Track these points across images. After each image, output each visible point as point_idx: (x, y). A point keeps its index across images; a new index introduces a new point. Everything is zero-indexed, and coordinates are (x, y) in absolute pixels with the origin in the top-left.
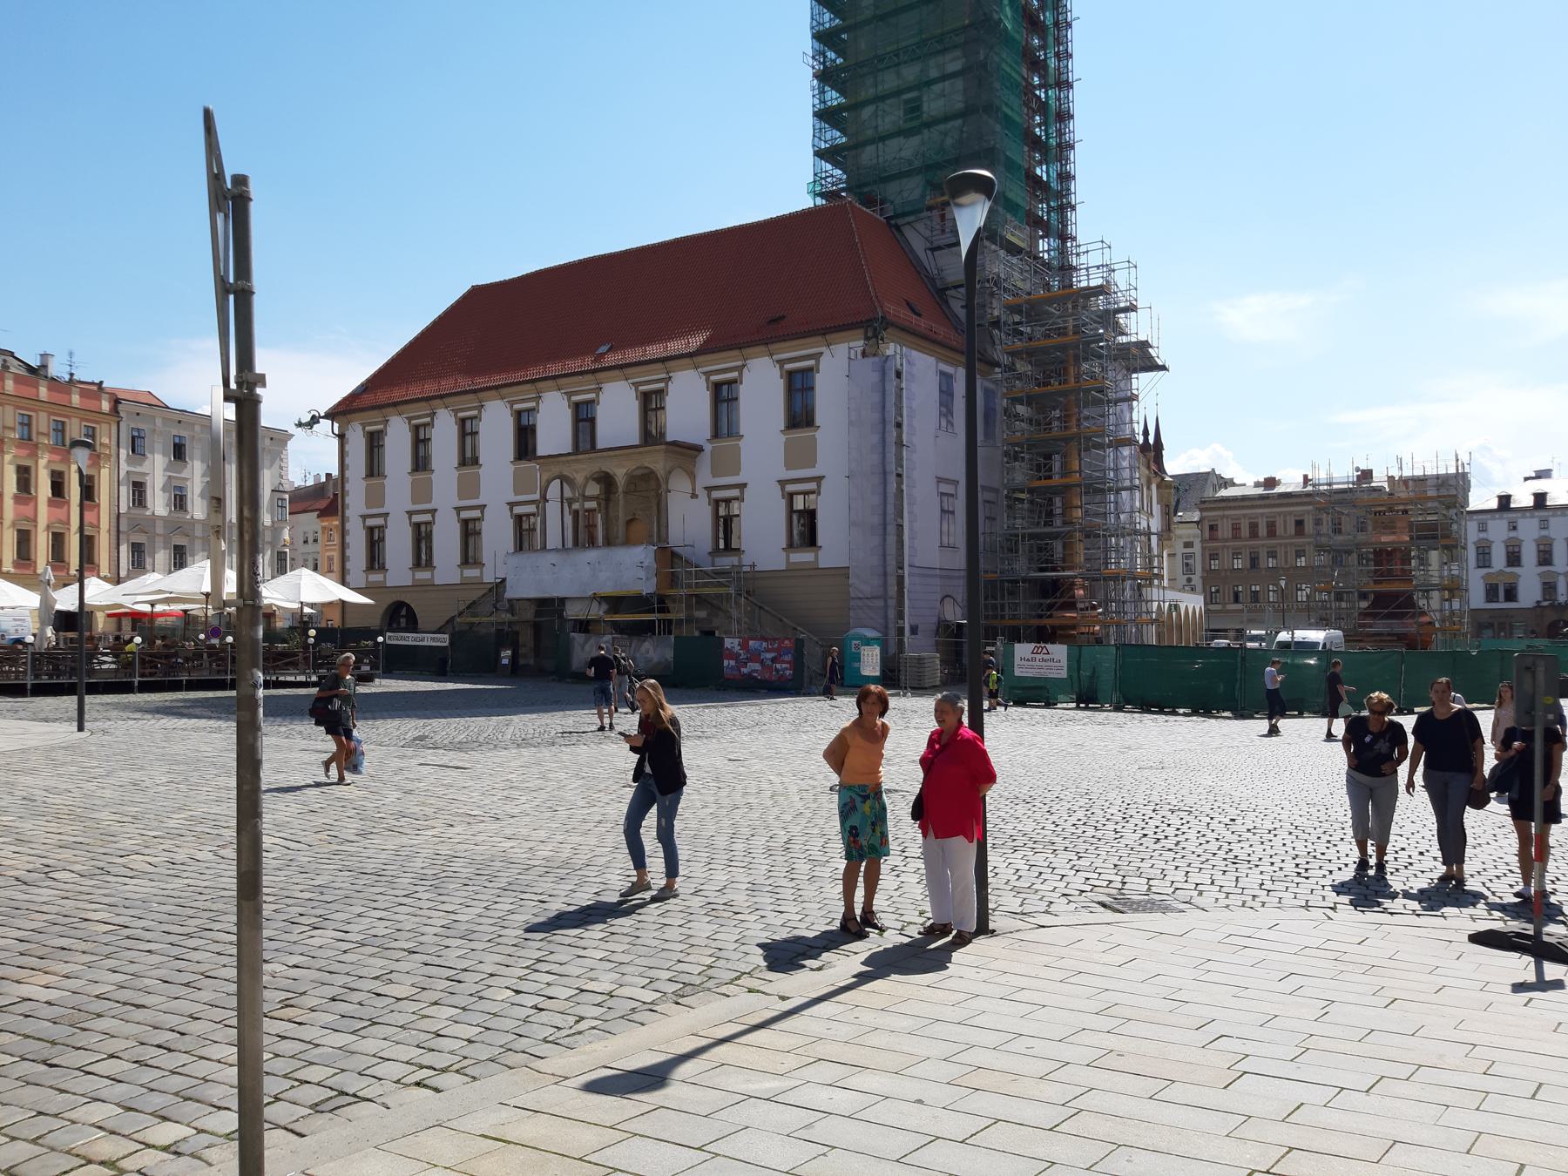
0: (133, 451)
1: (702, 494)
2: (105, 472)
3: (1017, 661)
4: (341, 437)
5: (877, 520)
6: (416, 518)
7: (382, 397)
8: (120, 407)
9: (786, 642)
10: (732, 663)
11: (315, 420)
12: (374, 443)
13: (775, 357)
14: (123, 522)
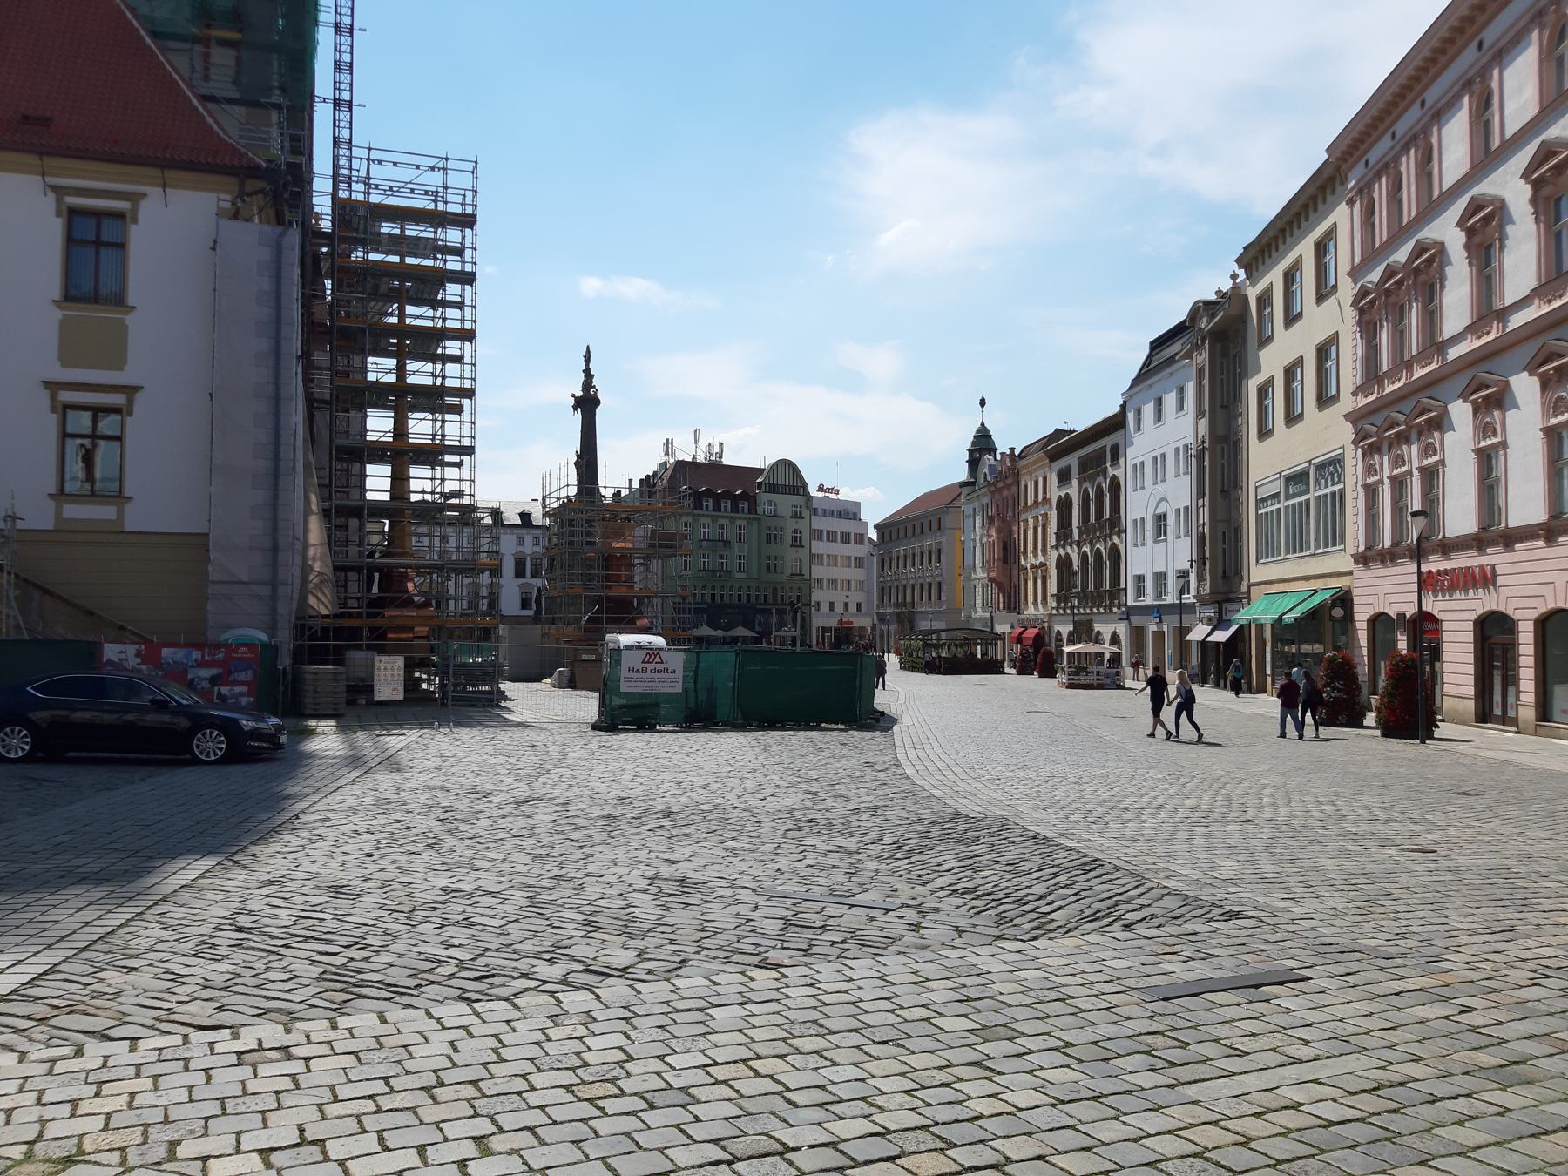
3: (624, 673)
9: (242, 650)
13: (48, 179)
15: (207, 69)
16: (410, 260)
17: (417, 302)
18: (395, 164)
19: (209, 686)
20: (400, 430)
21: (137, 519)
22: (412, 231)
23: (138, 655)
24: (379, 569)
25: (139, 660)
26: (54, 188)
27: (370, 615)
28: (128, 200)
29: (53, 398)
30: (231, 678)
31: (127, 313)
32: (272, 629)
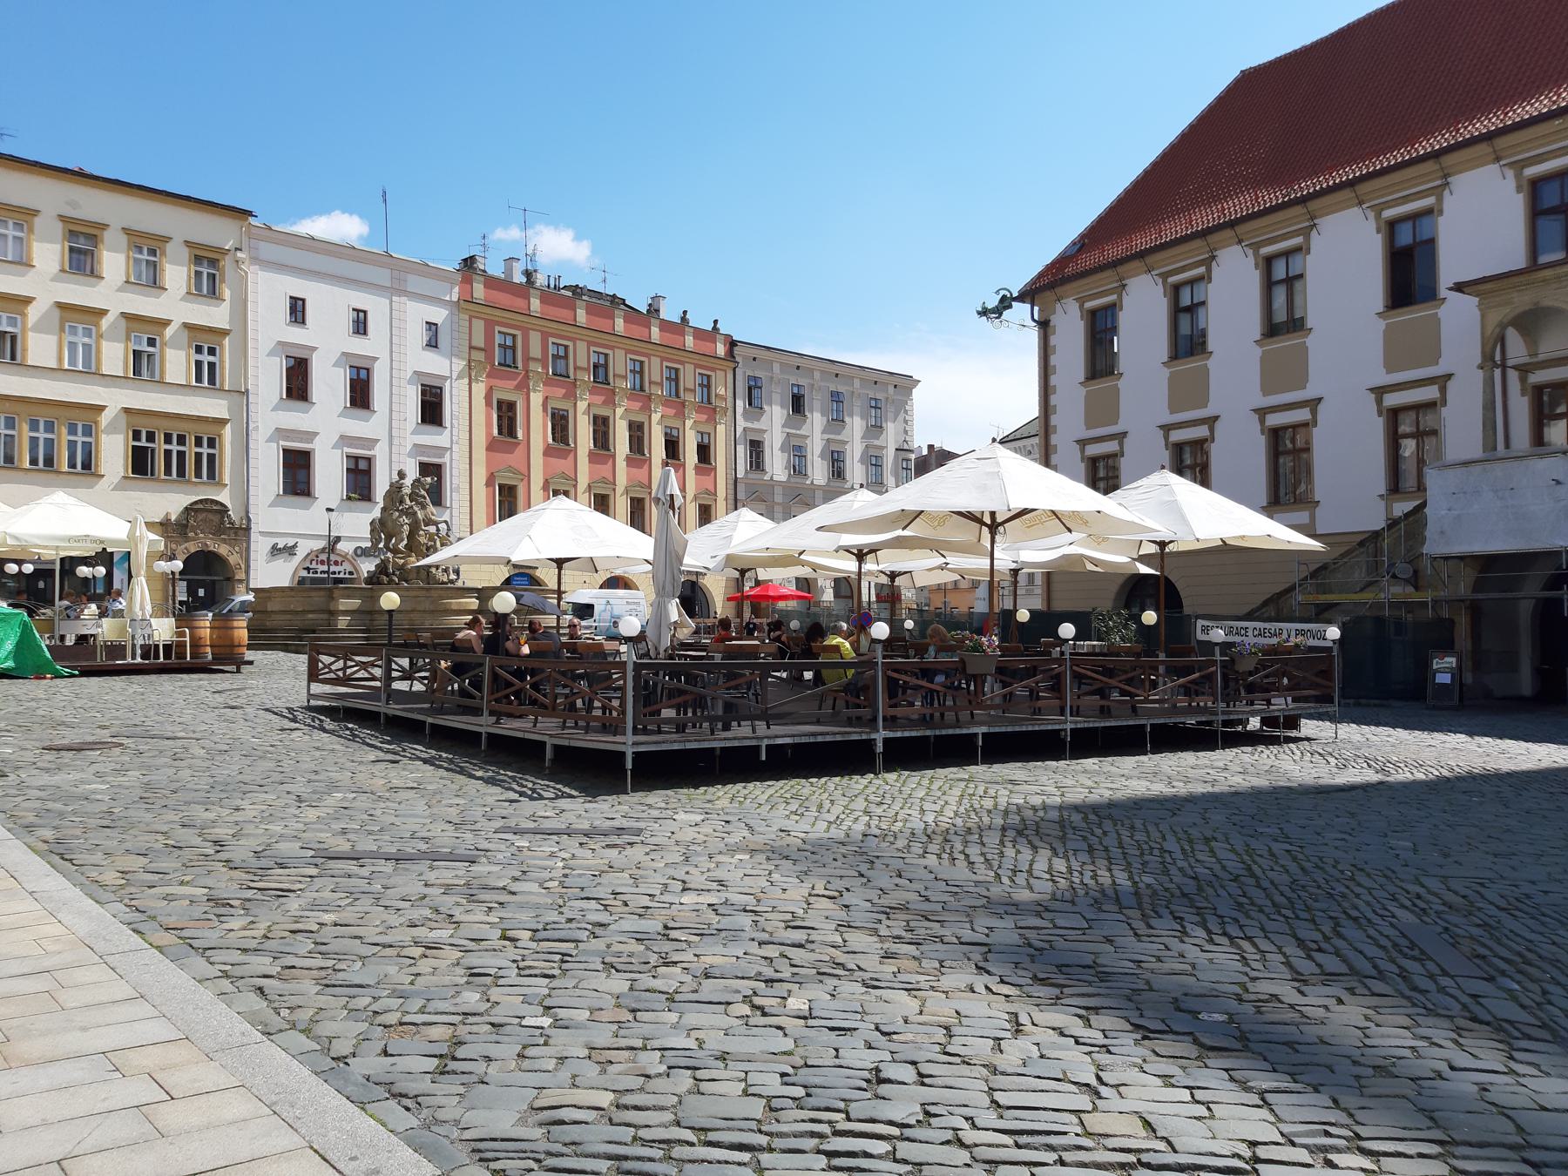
0: (750, 404)
2: (721, 429)
4: (1044, 325)
6: (1177, 436)
7: (1113, 251)
8: (737, 350)
11: (1005, 303)
12: (1101, 329)
14: (741, 487)
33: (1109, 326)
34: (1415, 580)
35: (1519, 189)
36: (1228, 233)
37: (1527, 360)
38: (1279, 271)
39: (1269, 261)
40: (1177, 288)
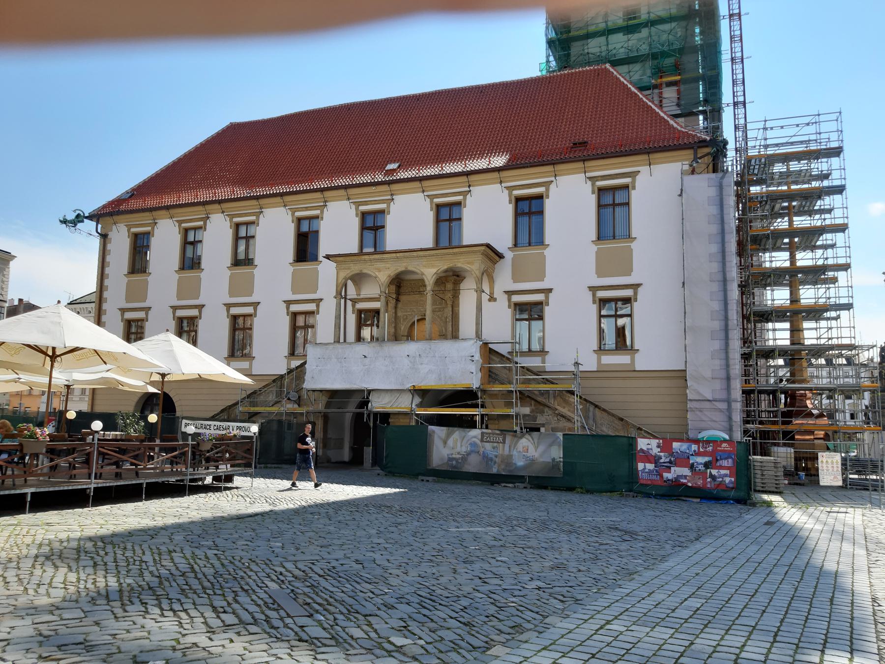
1: (502, 300)
4: (104, 237)
5: (717, 325)
6: (180, 313)
7: (151, 202)
9: (724, 445)
10: (650, 466)
11: (79, 219)
15: (661, 101)
16: (793, 187)
17: (800, 213)
18: (782, 127)
19: (703, 468)
20: (794, 299)
21: (642, 363)
22: (794, 166)
23: (658, 447)
24: (785, 392)
25: (659, 450)
26: (590, 178)
27: (784, 423)
28: (630, 177)
29: (594, 295)
30: (718, 464)
31: (632, 242)
32: (730, 431)
33: (145, 244)
34: (299, 402)
35: (357, 215)
36: (217, 206)
37: (356, 297)
38: (243, 232)
39: (238, 226)
40: (186, 231)
